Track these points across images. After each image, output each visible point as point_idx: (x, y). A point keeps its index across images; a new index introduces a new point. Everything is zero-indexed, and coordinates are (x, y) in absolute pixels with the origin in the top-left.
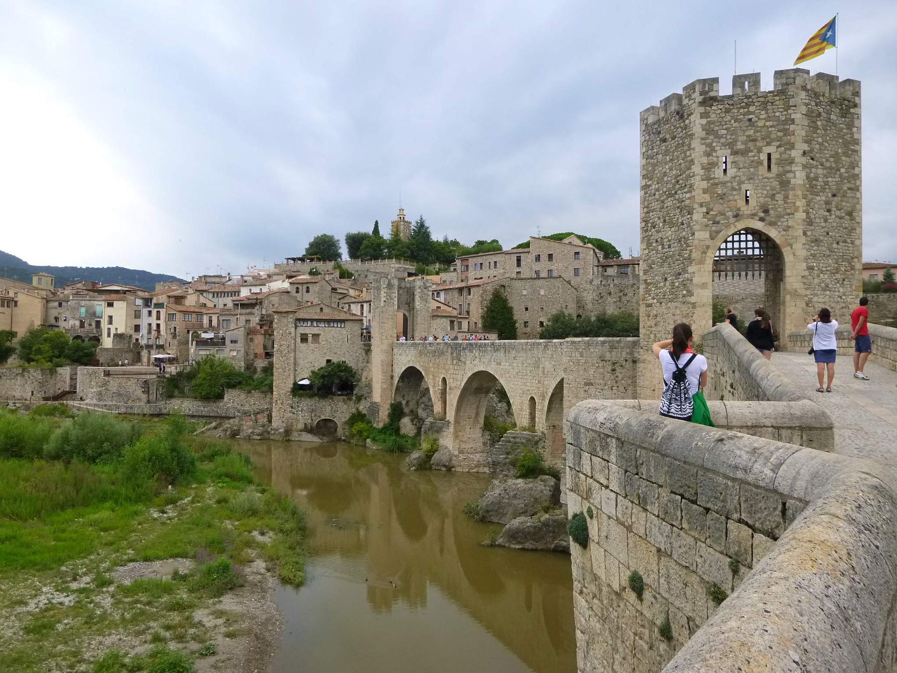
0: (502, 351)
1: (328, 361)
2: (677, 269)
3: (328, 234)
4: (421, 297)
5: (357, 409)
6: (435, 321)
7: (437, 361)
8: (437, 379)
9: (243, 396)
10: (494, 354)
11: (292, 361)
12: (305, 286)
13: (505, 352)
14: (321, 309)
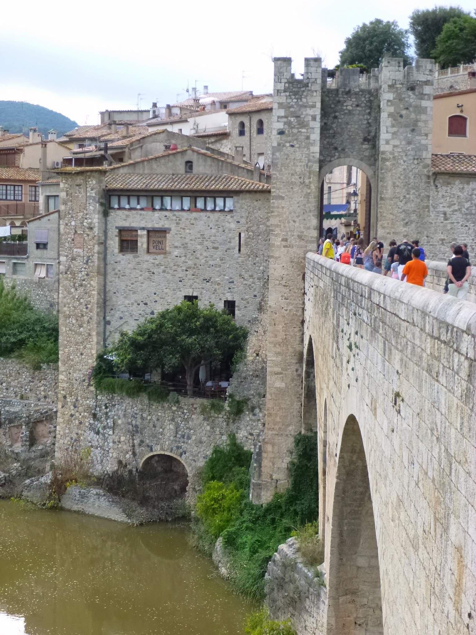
1: (191, 299)
3: (385, 19)
4: (396, 117)
5: (232, 437)
6: (443, 190)
9: (26, 376)
11: (95, 297)
12: (255, 119)
14: (189, 164)
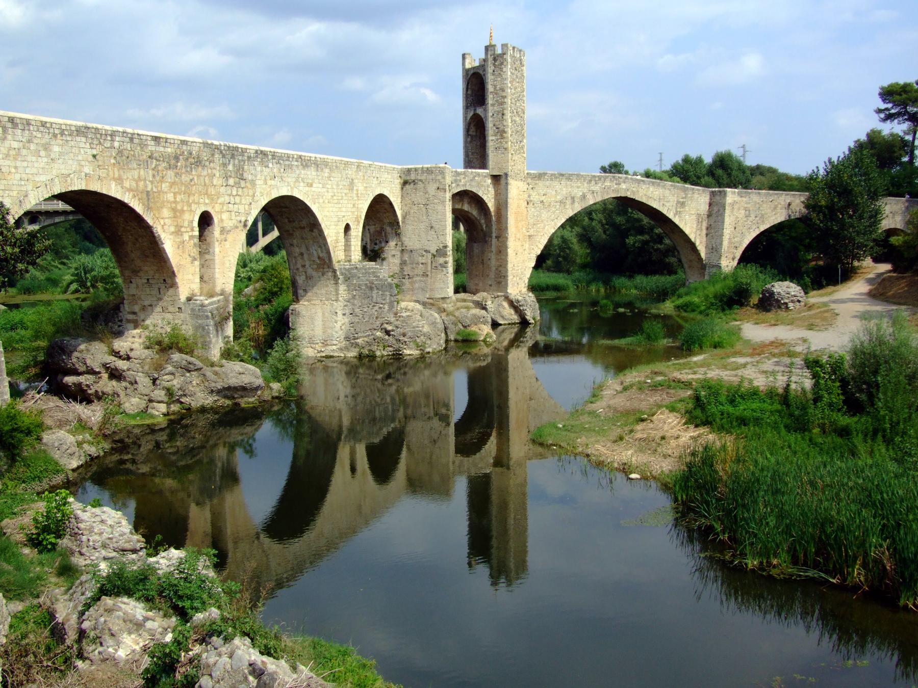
0: (313, 169)
2: (520, 139)
7: (185, 178)
8: (187, 216)
10: (303, 172)
13: (317, 170)
